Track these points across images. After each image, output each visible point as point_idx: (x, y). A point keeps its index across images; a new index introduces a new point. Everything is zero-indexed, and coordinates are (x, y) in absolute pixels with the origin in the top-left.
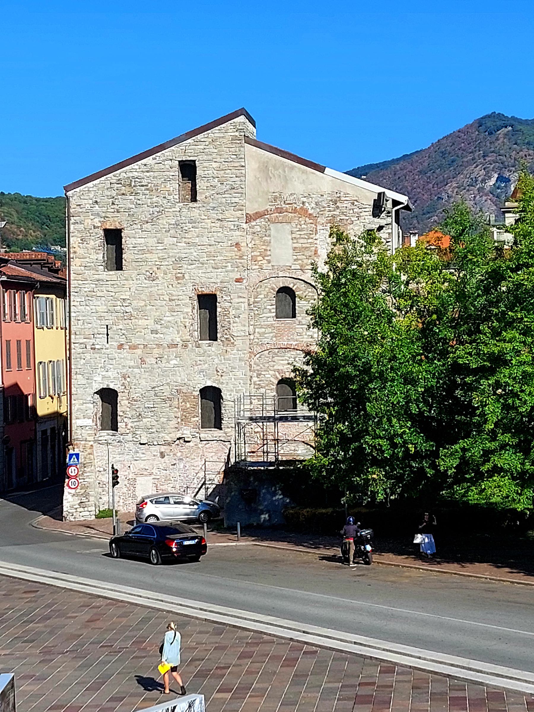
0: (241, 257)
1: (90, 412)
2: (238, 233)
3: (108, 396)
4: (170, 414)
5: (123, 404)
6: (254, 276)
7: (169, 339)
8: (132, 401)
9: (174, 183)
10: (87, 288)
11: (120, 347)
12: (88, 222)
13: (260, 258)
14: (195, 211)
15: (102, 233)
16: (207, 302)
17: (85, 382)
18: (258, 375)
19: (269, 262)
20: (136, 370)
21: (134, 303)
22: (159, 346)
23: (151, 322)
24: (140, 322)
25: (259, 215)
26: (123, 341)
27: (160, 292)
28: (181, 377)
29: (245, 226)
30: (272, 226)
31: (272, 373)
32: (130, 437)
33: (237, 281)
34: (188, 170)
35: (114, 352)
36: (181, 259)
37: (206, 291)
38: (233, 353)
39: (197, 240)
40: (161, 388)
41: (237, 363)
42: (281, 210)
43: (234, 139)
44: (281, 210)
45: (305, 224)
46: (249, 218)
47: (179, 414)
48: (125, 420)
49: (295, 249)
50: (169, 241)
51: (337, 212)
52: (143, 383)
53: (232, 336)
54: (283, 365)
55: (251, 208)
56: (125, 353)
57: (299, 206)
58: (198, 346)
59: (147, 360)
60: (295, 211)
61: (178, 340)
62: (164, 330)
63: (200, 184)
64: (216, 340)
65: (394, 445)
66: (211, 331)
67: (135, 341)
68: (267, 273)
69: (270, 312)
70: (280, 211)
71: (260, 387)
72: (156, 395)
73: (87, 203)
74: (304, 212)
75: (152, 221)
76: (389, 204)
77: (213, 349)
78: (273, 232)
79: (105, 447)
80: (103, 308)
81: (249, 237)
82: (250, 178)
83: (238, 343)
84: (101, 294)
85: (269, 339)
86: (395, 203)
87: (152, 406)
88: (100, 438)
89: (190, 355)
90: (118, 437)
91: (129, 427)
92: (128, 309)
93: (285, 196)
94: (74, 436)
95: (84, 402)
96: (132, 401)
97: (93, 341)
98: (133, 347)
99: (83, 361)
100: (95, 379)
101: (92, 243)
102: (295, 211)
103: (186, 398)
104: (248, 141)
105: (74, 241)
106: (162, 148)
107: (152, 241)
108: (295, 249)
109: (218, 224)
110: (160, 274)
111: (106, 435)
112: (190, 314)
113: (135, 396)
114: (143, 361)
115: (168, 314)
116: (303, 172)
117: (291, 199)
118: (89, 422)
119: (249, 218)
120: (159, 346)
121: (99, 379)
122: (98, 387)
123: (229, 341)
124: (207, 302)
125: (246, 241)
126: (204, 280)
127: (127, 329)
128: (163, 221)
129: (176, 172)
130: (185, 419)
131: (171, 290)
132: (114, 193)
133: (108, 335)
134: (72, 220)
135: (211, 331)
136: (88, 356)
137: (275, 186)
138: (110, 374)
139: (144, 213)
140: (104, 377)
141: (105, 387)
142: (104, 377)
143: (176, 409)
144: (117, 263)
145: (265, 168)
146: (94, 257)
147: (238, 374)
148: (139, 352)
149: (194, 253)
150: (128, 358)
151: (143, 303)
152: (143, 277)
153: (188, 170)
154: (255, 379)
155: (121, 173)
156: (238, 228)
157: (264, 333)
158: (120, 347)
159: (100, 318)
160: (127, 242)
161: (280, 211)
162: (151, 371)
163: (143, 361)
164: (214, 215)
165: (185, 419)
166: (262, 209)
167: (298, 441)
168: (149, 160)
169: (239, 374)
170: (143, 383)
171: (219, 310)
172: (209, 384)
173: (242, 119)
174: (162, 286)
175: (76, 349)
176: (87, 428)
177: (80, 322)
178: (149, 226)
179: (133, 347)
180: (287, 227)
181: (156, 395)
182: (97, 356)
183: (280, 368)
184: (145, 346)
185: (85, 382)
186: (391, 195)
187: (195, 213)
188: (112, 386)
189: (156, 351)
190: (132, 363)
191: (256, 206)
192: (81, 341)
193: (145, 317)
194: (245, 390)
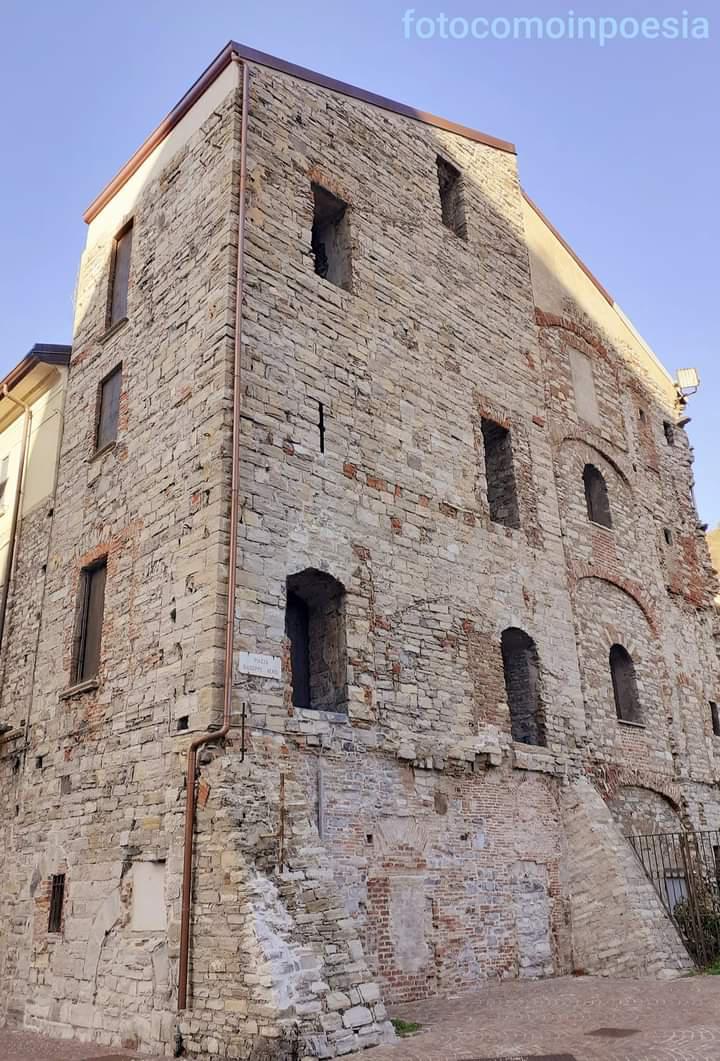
28: (466, 592)
32: (371, 737)
40: (433, 607)
48: (365, 679)
72: (423, 622)
87: (417, 651)
88: (304, 728)
91: (374, 701)
95: (263, 598)
100: (293, 535)
111: (314, 722)
121: (304, 540)
122: (297, 563)
141: (317, 567)
143: (464, 673)
172: (516, 624)
176: (267, 686)
181: (423, 622)
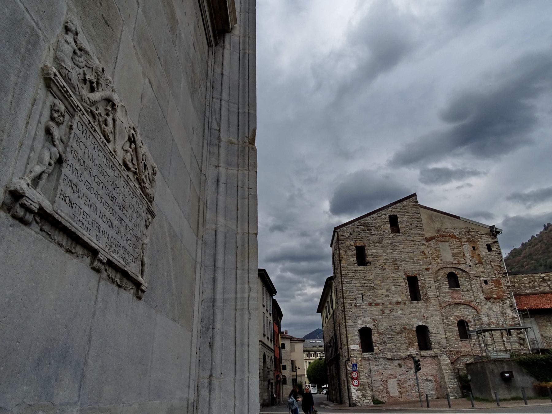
0: (426, 258)
2: (423, 247)
4: (402, 341)
6: (435, 267)
7: (395, 299)
11: (370, 304)
13: (436, 258)
16: (413, 282)
17: (352, 324)
18: (447, 319)
19: (441, 260)
20: (380, 317)
21: (375, 282)
22: (390, 303)
23: (384, 292)
24: (379, 291)
25: (432, 238)
26: (371, 301)
27: (388, 276)
28: (405, 320)
29: (425, 243)
31: (453, 317)
35: (366, 307)
36: (396, 259)
39: (403, 250)
41: (434, 313)
45: (455, 241)
46: (427, 240)
47: (407, 341)
49: (453, 254)
50: (388, 251)
51: (470, 237)
52: (384, 324)
53: (429, 298)
54: (459, 313)
55: (428, 235)
56: (373, 308)
58: (411, 304)
59: (385, 311)
60: (449, 236)
61: (400, 300)
62: (392, 295)
67: (378, 301)
68: (441, 266)
69: (446, 285)
71: (448, 325)
74: (454, 236)
75: (380, 241)
77: (420, 305)
78: (440, 246)
80: (359, 285)
81: (429, 249)
83: (433, 301)
84: (356, 277)
92: (372, 285)
96: (380, 334)
97: (355, 301)
98: (377, 304)
99: (351, 313)
101: (350, 253)
102: (449, 236)
107: (381, 251)
108: (453, 254)
109: (412, 243)
110: (387, 267)
114: (383, 312)
115: (393, 287)
116: (450, 219)
120: (390, 303)
122: (359, 327)
123: (427, 300)
124: (413, 282)
125: (428, 251)
126: (409, 270)
127: (373, 295)
128: (385, 242)
130: (411, 345)
131: (393, 275)
132: (359, 230)
133: (363, 298)
137: (437, 225)
138: (366, 319)
140: (363, 321)
142: (363, 321)
146: (352, 259)
147: (436, 318)
148: (380, 307)
149: (402, 257)
150: (375, 311)
151: (379, 282)
152: (377, 269)
154: (445, 321)
156: (423, 245)
157: (445, 296)
158: (370, 304)
159: (358, 290)
162: (388, 317)
163: (383, 312)
166: (433, 235)
170: (384, 324)
171: (419, 284)
172: (421, 324)
174: (387, 273)
177: (348, 292)
179: (377, 304)
180: (447, 244)
181: (392, 330)
182: (358, 310)
183: (458, 314)
184: (383, 304)
185: (352, 324)
187: (400, 238)
189: (389, 306)
190: (377, 313)
191: (430, 234)
192: (349, 302)
193: (382, 289)
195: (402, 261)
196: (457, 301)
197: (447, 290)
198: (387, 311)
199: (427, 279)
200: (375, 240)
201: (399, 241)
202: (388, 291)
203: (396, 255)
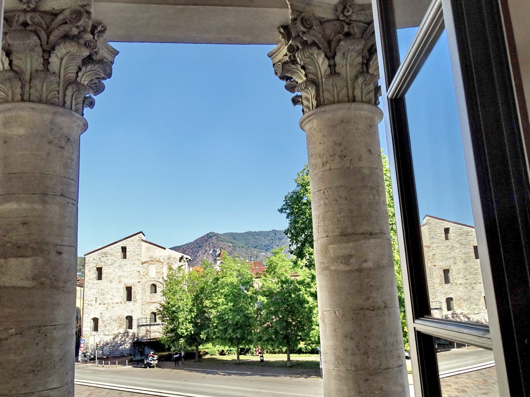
1: (89, 326)
3: (96, 320)
5: (100, 323)
6: (144, 281)
8: (103, 321)
9: (120, 254)
10: (91, 285)
11: (100, 304)
12: (91, 266)
14: (125, 261)
15: (96, 269)
16: (129, 290)
21: (105, 290)
25: (146, 262)
26: (101, 302)
28: (120, 313)
30: (150, 266)
32: (102, 333)
33: (139, 282)
34: (124, 249)
37: (129, 286)
38: (137, 304)
42: (152, 261)
43: (139, 240)
44: (152, 261)
45: (160, 265)
46: (143, 263)
50: (117, 270)
52: (107, 316)
56: (102, 306)
57: (158, 259)
63: (128, 254)
64: (131, 300)
65: (187, 331)
66: (129, 298)
67: (105, 302)
70: (152, 261)
71: (145, 315)
73: (91, 260)
74: (159, 261)
76: (185, 259)
79: (93, 337)
82: (143, 252)
83: (138, 301)
85: (148, 300)
86: (187, 259)
89: (123, 306)
90: (98, 333)
93: (154, 256)
94: (83, 334)
96: (103, 321)
98: (104, 304)
103: (121, 319)
104: (143, 240)
105: (86, 271)
106: (116, 243)
107: (112, 271)
110: (114, 281)
111: (94, 333)
112: (124, 294)
113: (104, 320)
114: (107, 308)
117: (155, 258)
118: (89, 329)
119: (143, 263)
123: (135, 301)
124: (129, 290)
128: (116, 265)
129: (120, 250)
130: (120, 327)
131: (117, 286)
134: (86, 265)
135: (129, 298)
136: (89, 307)
137: (151, 254)
139: (109, 262)
144: (100, 277)
145: (148, 249)
146: (93, 276)
148: (106, 305)
149: (125, 274)
150: (103, 307)
153: (124, 249)
155: (103, 250)
158: (100, 304)
160: (104, 271)
161: (152, 261)
162: (110, 312)
163: (107, 308)
164: (131, 262)
165: (120, 327)
167: (157, 332)
168: (112, 246)
169: (139, 311)
170: (107, 316)
173: (141, 234)
174: (114, 284)
175: (85, 305)
178: (110, 266)
179: (104, 304)
180: (154, 266)
186: (185, 256)
188: (97, 317)
193: (109, 294)
194: (140, 316)
195: (124, 277)
196: (153, 301)
197: (149, 294)
198: (110, 308)
199: (138, 288)
200: (109, 264)
201: (125, 265)
202: (112, 296)
203: (121, 273)
